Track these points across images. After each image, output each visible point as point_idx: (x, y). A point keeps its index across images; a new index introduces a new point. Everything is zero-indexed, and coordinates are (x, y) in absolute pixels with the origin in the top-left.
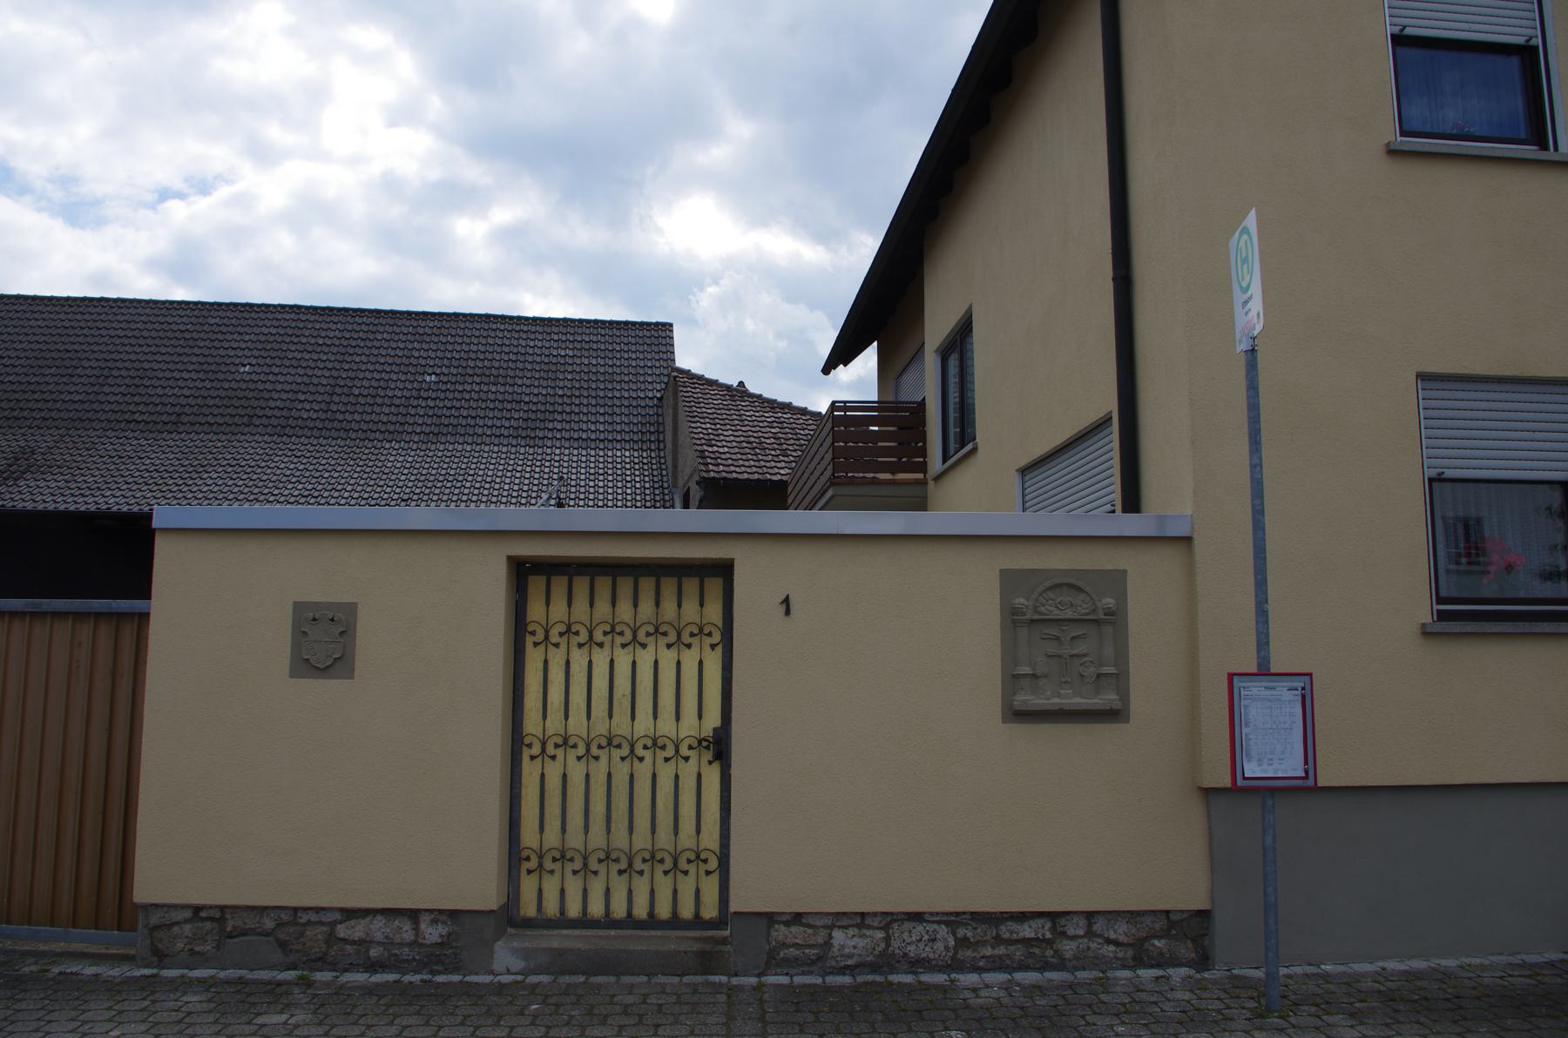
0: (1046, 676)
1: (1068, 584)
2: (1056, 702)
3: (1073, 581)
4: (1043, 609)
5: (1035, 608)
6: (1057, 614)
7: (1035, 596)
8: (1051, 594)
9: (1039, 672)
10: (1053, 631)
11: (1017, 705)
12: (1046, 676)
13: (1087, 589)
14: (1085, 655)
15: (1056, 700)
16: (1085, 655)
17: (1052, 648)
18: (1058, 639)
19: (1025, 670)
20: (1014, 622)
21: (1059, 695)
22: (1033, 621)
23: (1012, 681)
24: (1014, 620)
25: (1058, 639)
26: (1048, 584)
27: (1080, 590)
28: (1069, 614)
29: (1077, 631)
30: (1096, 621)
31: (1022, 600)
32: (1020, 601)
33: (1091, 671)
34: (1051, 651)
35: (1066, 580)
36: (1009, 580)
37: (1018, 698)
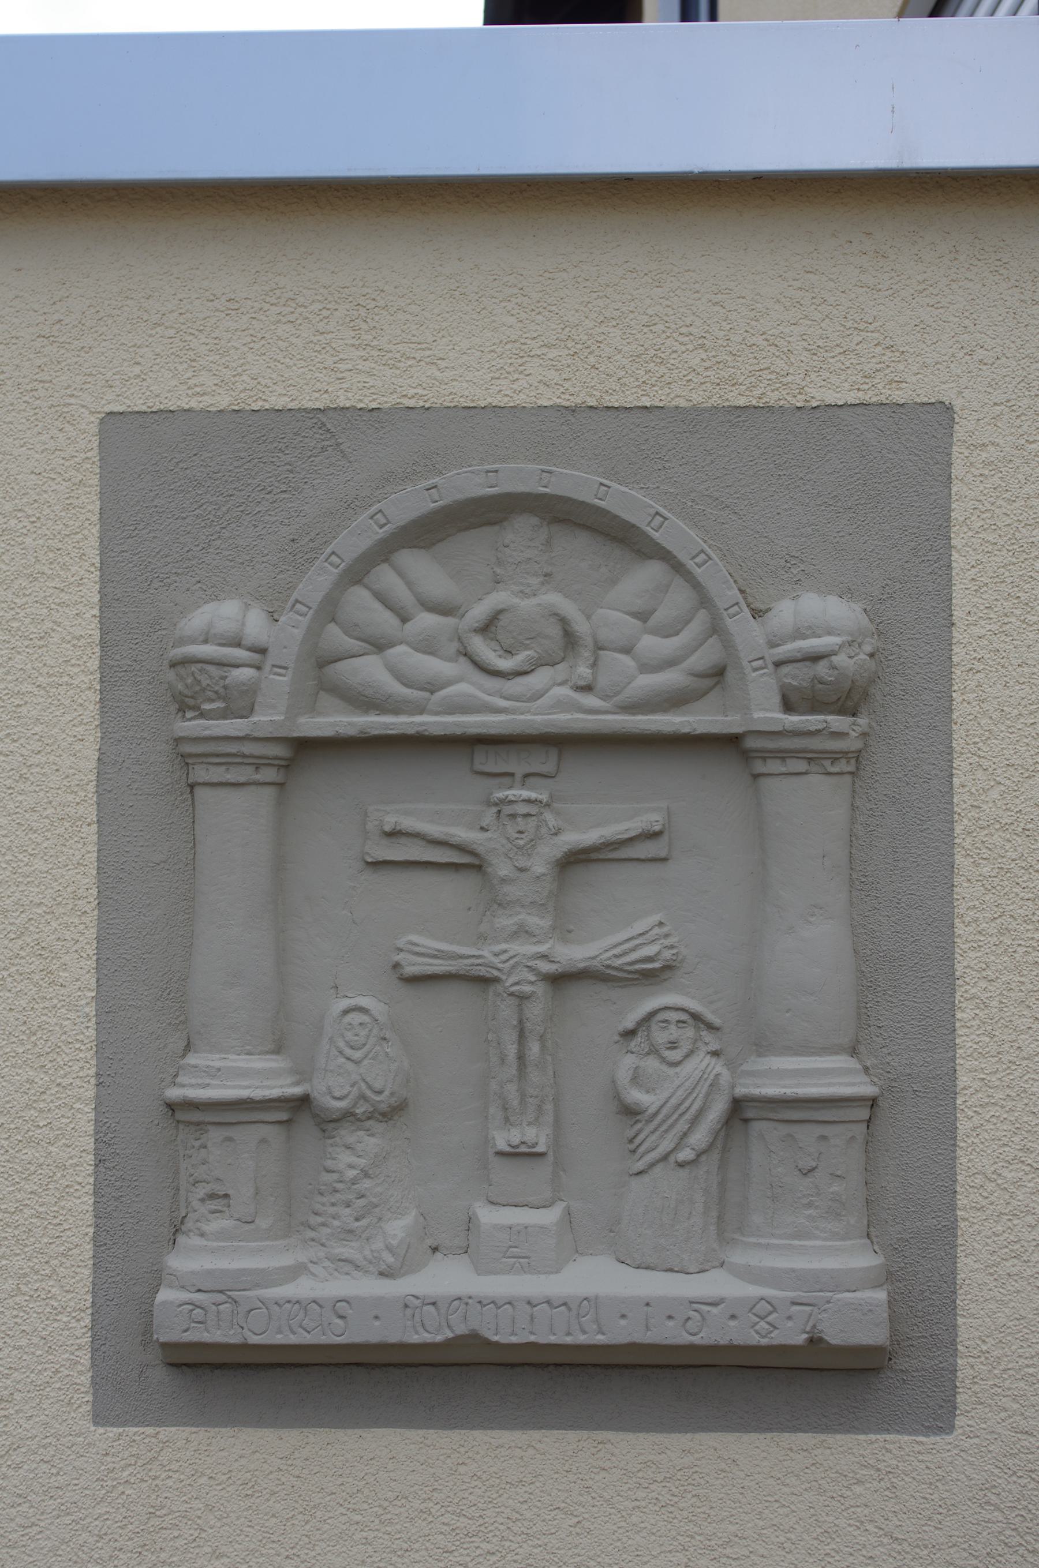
0: (392, 1113)
1: (524, 509)
2: (448, 1290)
3: (576, 481)
4: (370, 671)
5: (320, 669)
6: (499, 710)
7: (316, 584)
8: (425, 572)
9: (332, 1089)
10: (440, 809)
11: (178, 1312)
12: (392, 1113)
13: (676, 534)
14: (651, 976)
15: (446, 1279)
16: (651, 976)
17: (431, 926)
18: (471, 864)
19: (235, 1071)
20: (185, 755)
21: (466, 1241)
22: (306, 749)
23: (163, 1144)
24: (223, 767)
25: (471, 864)
26: (408, 503)
27: (624, 538)
28: (549, 701)
29: (600, 809)
30: (730, 744)
31: (225, 613)
32: (222, 616)
33: (685, 1081)
34: (428, 947)
35: (520, 476)
36: (171, 483)
37: (189, 1260)
